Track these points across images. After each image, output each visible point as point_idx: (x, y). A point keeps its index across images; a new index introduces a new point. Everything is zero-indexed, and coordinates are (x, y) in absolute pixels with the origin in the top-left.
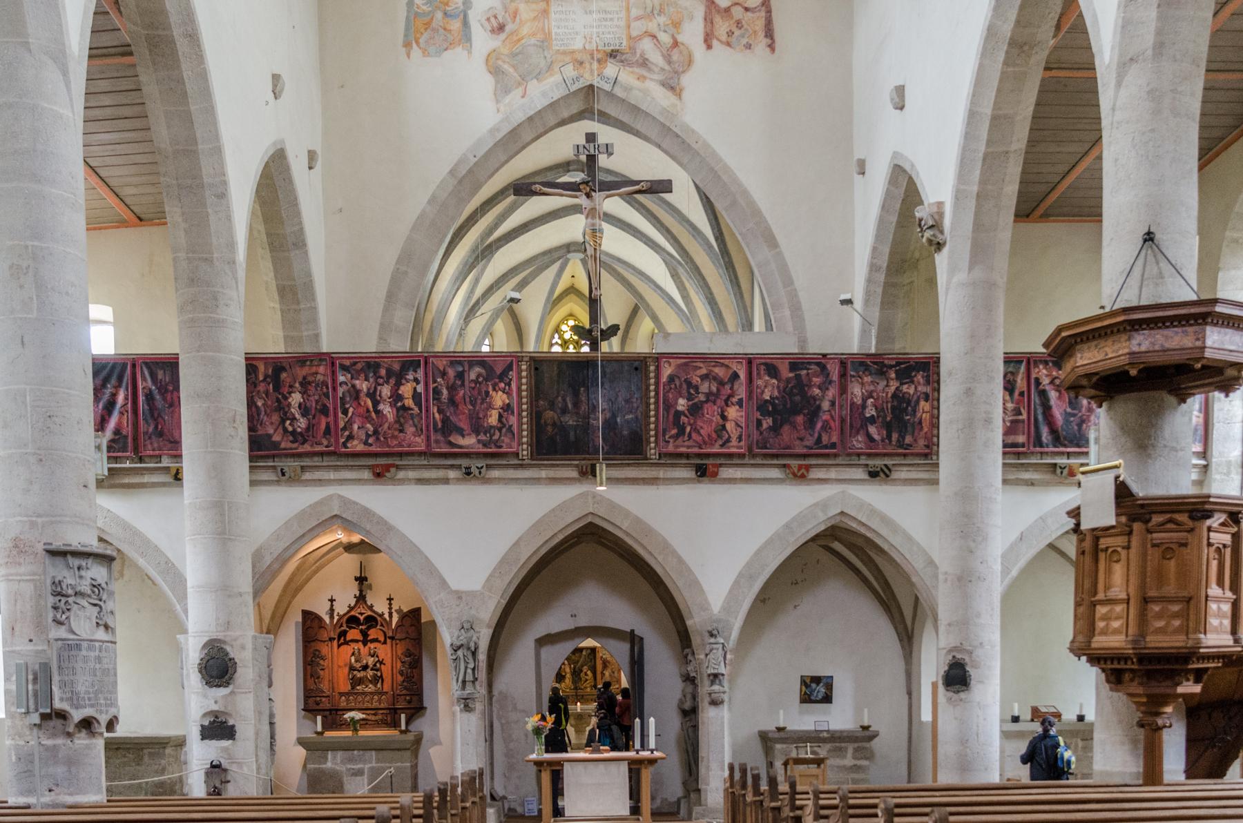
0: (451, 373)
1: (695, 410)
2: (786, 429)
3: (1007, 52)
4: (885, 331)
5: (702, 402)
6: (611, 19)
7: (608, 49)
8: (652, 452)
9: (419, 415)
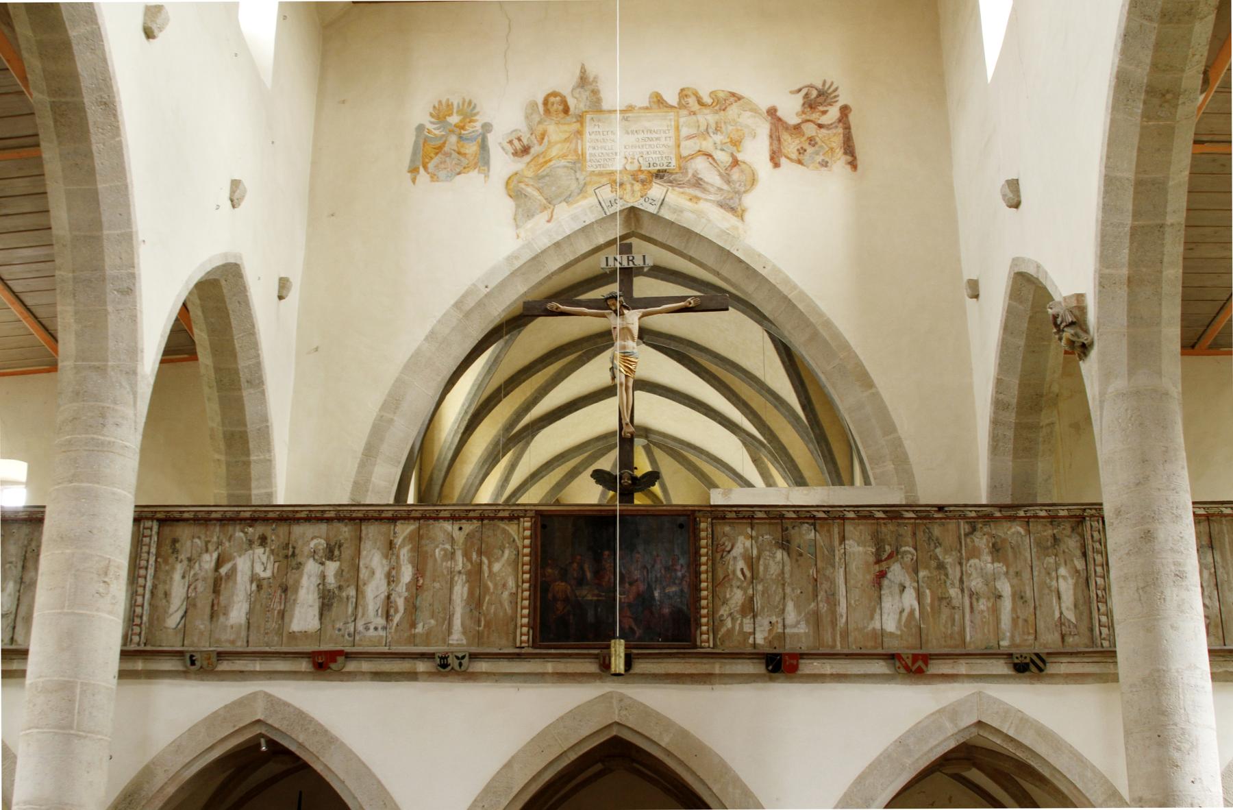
4: (1024, 480)
6: (657, 139)
7: (654, 169)
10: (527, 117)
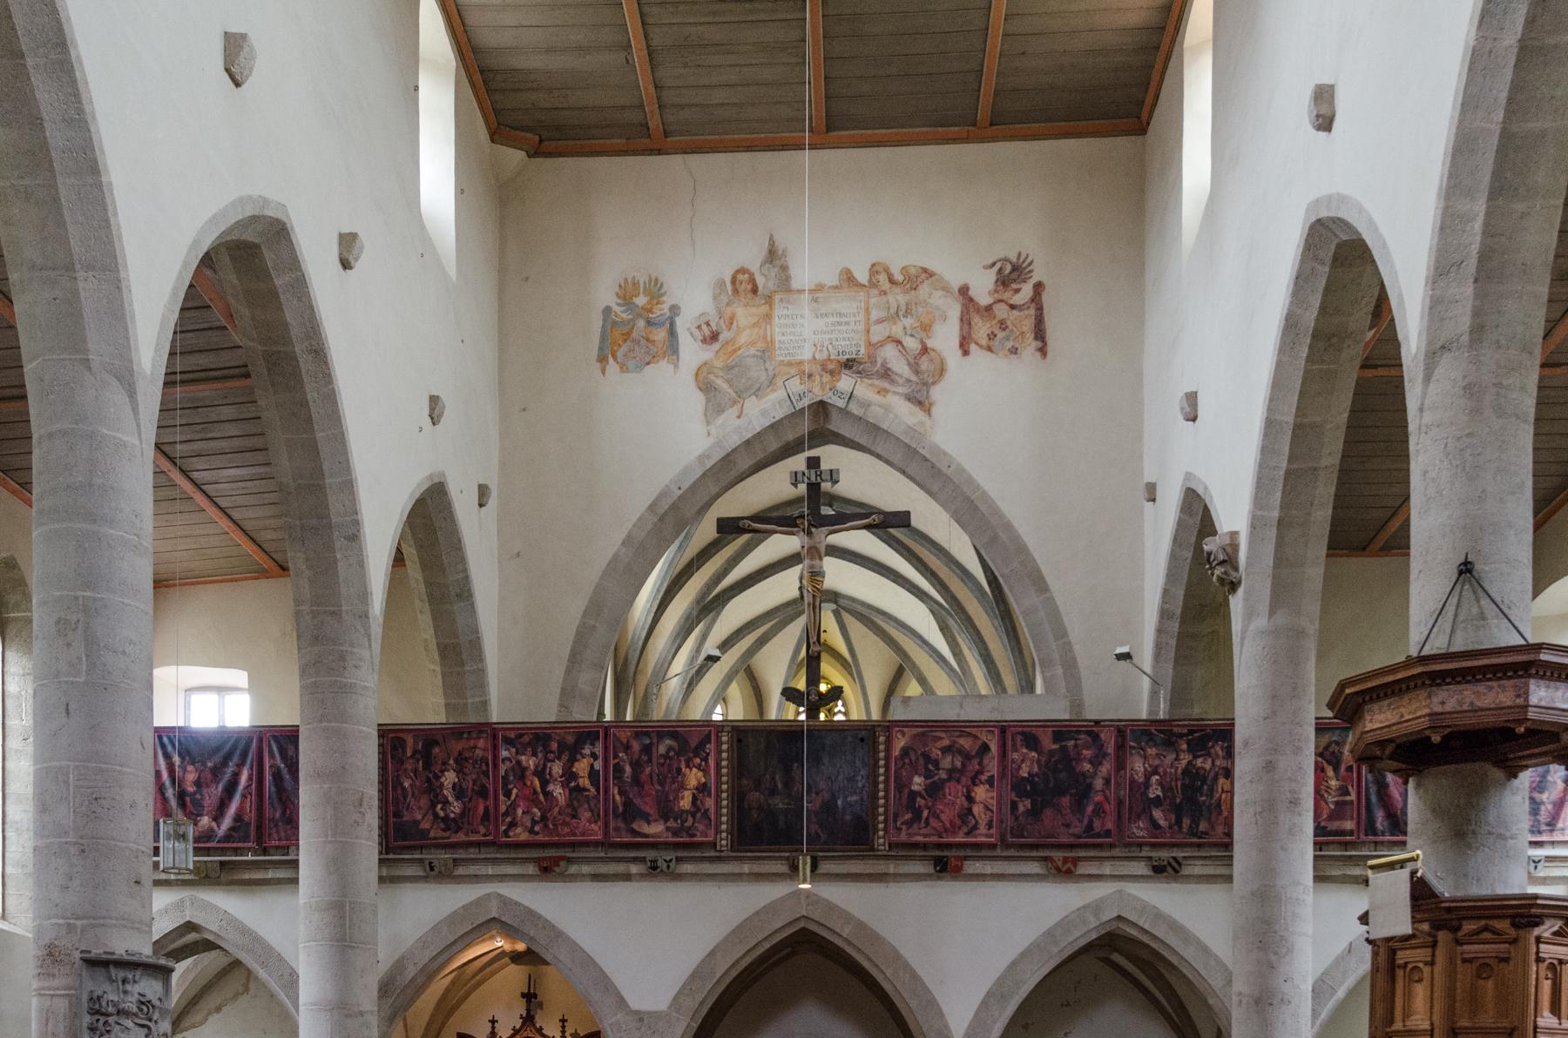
0: (636, 746)
1: (934, 790)
2: (1048, 812)
3: (1310, 347)
5: (943, 781)
6: (847, 323)
7: (843, 358)
8: (880, 842)
9: (596, 797)
10: (715, 298)
